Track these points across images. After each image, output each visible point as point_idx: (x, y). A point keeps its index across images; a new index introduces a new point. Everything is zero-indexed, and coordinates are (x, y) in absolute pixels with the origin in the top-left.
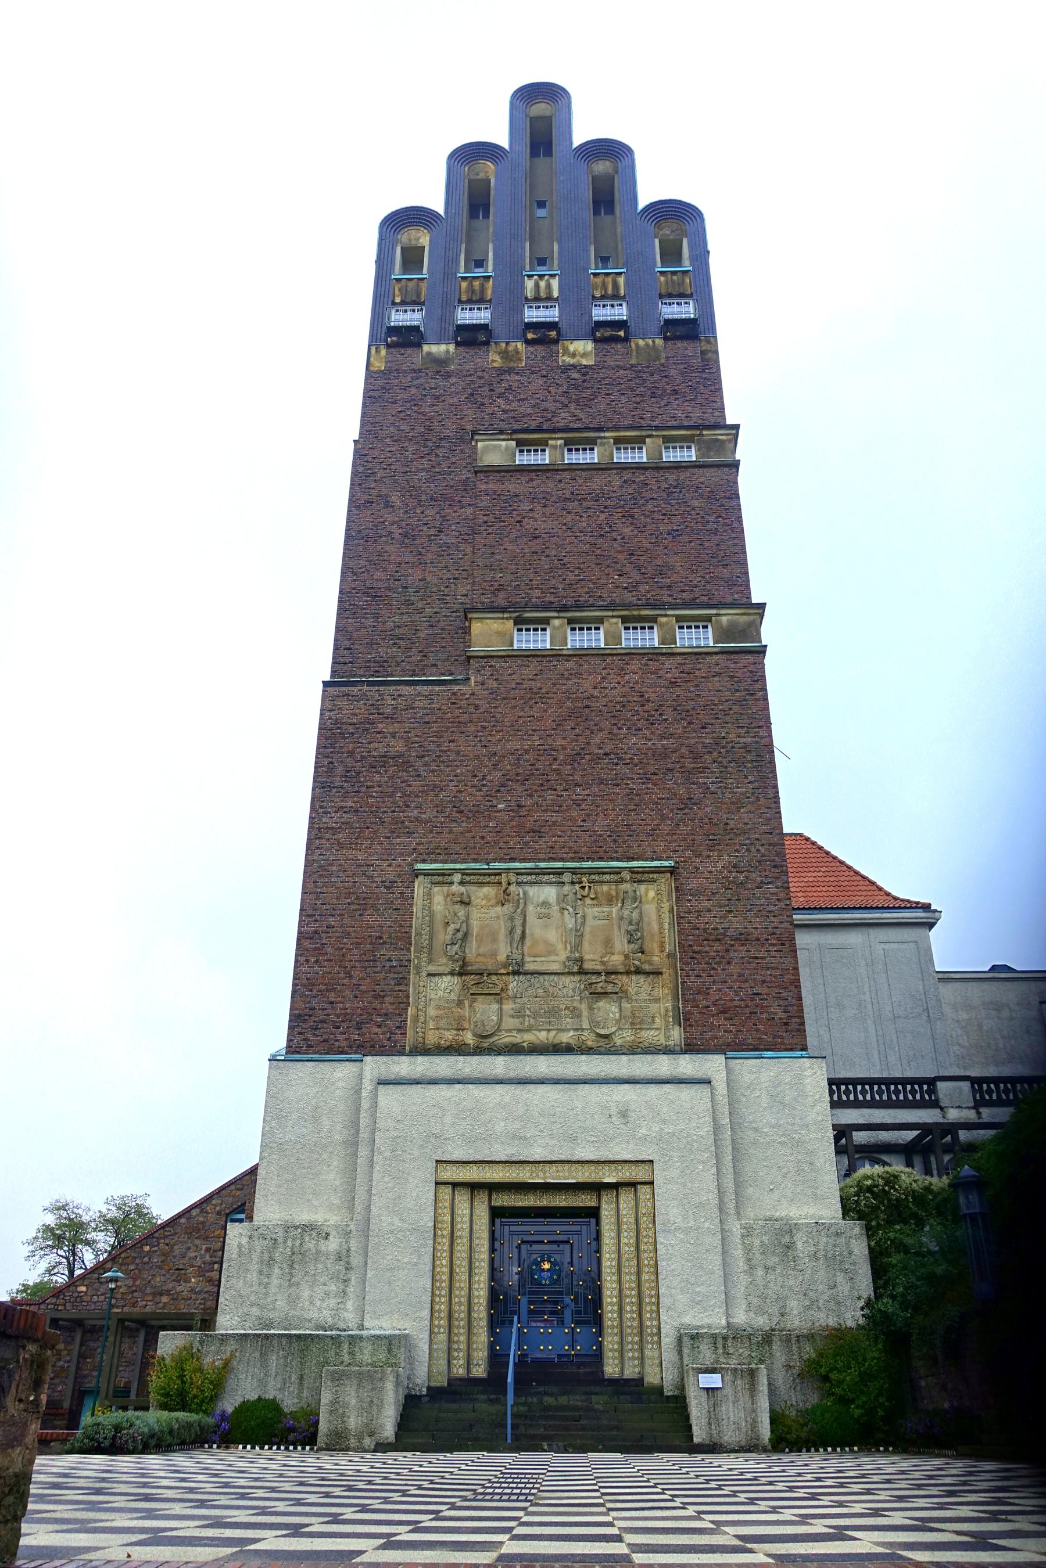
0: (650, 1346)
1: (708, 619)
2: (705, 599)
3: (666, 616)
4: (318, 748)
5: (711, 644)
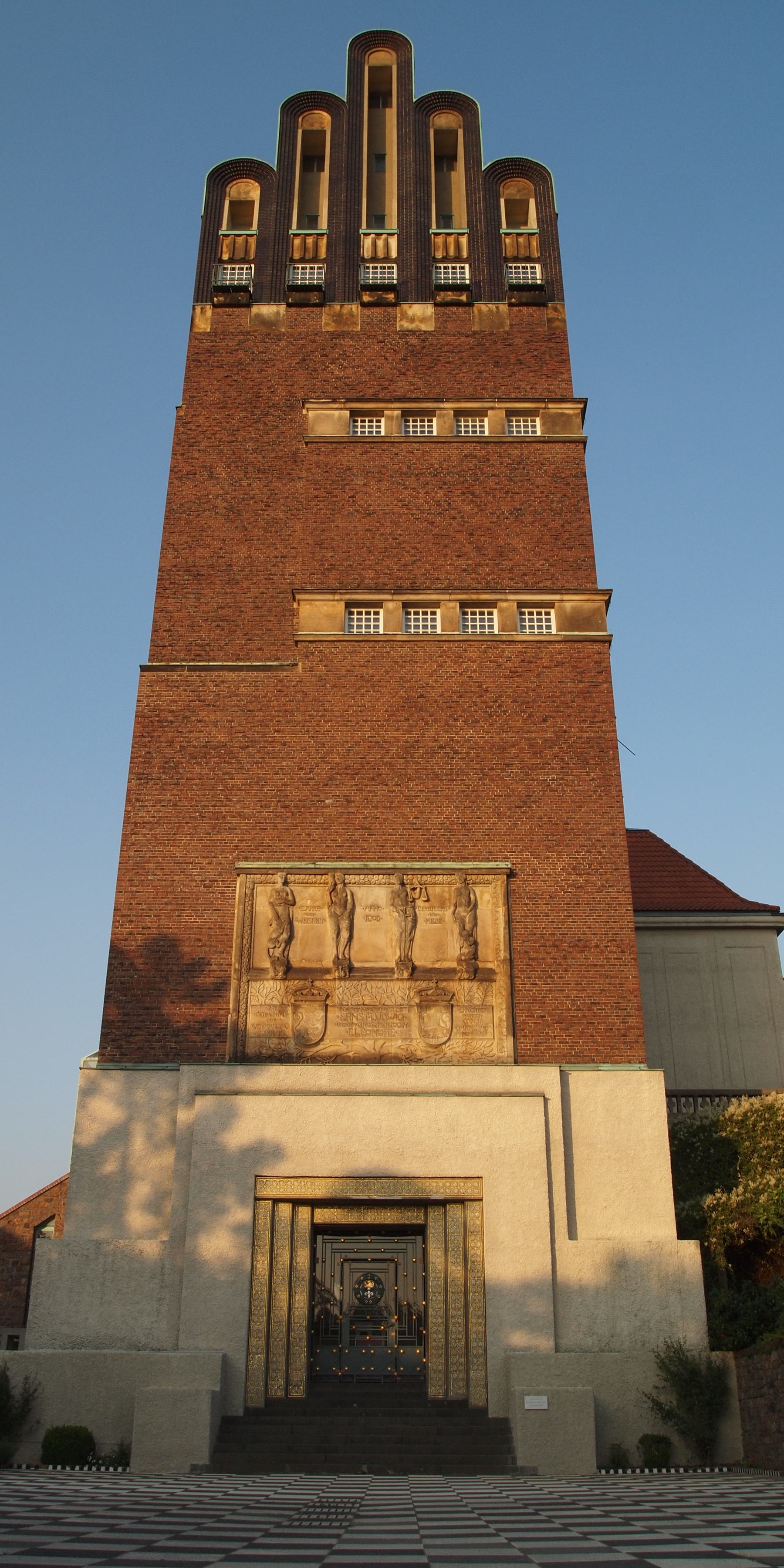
2: (548, 583)
3: (506, 600)
4: (134, 737)
5: (554, 631)
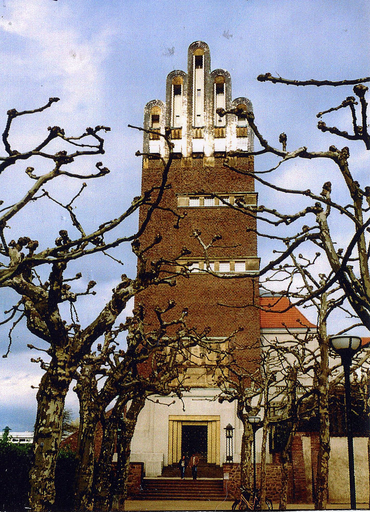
1: (244, 262)
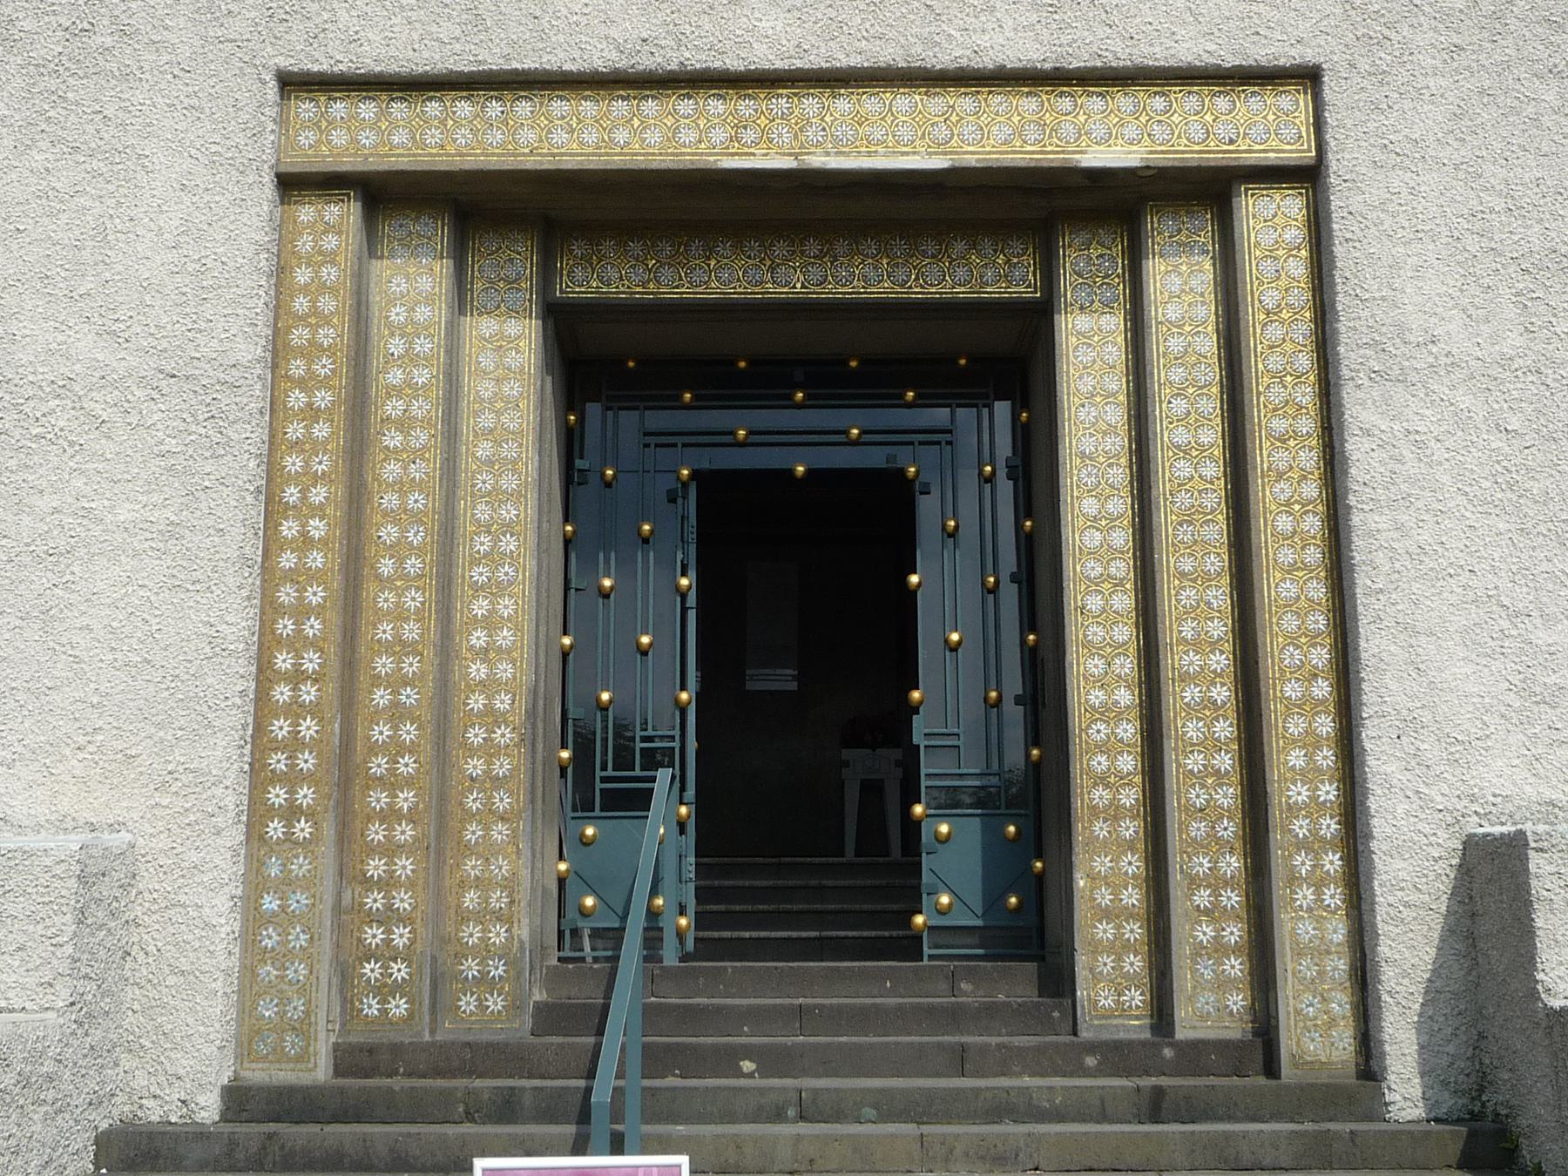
0: (1305, 895)
